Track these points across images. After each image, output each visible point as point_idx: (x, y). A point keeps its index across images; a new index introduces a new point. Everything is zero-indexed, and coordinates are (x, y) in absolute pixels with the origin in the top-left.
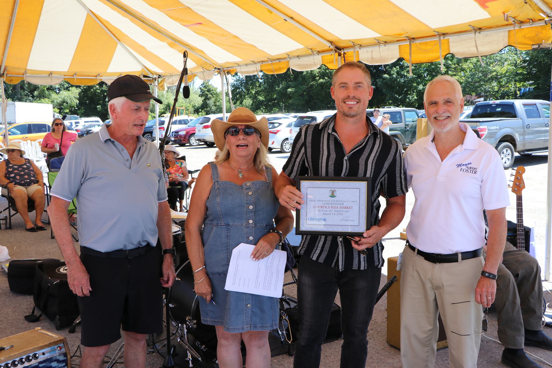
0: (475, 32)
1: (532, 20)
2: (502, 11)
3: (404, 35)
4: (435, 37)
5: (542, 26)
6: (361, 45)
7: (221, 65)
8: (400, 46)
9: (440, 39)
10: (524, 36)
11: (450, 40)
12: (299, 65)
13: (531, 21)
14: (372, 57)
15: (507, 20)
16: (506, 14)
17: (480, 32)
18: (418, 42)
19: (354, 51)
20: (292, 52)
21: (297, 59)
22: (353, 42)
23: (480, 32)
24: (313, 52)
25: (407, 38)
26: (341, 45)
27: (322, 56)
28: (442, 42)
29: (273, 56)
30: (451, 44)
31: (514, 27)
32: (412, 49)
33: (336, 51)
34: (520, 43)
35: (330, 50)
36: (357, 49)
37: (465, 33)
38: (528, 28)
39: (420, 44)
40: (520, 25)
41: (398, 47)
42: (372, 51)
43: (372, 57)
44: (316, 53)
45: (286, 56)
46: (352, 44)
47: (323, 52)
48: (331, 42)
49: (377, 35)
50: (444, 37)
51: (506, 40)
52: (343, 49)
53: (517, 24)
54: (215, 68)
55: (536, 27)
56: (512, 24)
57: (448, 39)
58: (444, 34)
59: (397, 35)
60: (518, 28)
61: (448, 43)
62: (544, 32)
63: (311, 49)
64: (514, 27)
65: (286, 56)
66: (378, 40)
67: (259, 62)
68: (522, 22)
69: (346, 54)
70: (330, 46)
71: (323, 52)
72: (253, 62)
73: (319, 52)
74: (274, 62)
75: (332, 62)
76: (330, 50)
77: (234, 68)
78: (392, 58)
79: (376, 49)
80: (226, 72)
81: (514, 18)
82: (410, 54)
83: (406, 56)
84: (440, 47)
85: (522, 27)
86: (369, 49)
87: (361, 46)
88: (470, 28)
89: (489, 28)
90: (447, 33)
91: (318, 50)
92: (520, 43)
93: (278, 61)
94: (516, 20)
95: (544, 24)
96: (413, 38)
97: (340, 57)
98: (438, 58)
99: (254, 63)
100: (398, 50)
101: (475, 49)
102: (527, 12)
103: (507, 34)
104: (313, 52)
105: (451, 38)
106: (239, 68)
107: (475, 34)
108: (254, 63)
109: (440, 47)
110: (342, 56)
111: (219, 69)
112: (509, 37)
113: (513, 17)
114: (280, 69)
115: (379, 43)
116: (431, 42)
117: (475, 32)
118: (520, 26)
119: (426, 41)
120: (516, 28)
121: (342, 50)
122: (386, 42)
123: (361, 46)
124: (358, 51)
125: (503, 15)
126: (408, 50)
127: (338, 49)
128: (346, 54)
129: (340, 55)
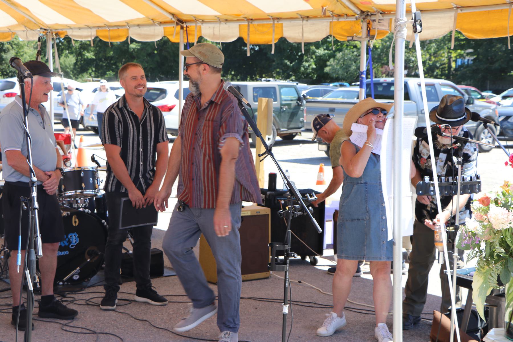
0: (303, 20)
1: (347, 15)
2: (321, 5)
3: (242, 16)
4: (268, 20)
5: (354, 21)
6: (203, 21)
7: (49, 26)
8: (240, 25)
9: (274, 23)
10: (342, 28)
11: (284, 25)
12: (139, 35)
13: (345, 16)
14: (214, 34)
15: (324, 13)
16: (324, 8)
17: (307, 20)
18: (255, 23)
19: (196, 26)
20: (132, 20)
21: (137, 28)
22: (195, 17)
23: (307, 20)
24: (153, 22)
25: (246, 19)
26: (184, 18)
27: (164, 28)
28: (275, 25)
29: (111, 23)
30: (284, 29)
32: (251, 30)
33: (177, 24)
34: (339, 34)
35: (171, 22)
36: (199, 24)
37: (297, 20)
38: (345, 21)
39: (258, 25)
40: (337, 18)
41: (238, 26)
42: (214, 28)
43: (214, 34)
44: (158, 24)
45: (126, 24)
46: (194, 19)
47: (165, 23)
48: (173, 15)
49: (217, 14)
50: (278, 22)
51: (328, 30)
52: (185, 22)
53: (335, 17)
54: (41, 28)
55: (351, 21)
56: (329, 16)
57: (282, 24)
58: (278, 19)
59: (235, 15)
60: (336, 20)
61: (282, 27)
62: (357, 26)
63: (152, 20)
64: (333, 19)
65: (126, 24)
66: (218, 18)
67: (94, 27)
68: (339, 16)
69: (188, 27)
70: (171, 19)
71: (165, 23)
72: (88, 26)
73: (161, 23)
74: (111, 28)
75: (172, 35)
76: (171, 22)
77: (64, 30)
78: (233, 37)
79: (217, 25)
80: (54, 34)
81: (332, 11)
82: (248, 35)
83: (245, 37)
84: (274, 30)
85: (340, 20)
86: (212, 25)
87: (203, 21)
88: (300, 17)
89: (315, 17)
90: (281, 18)
91: (160, 20)
92: (339, 34)
93: (116, 28)
95: (355, 19)
96: (252, 19)
97: (182, 31)
98: (271, 41)
99: (89, 27)
100: (237, 29)
101: (301, 35)
102: (339, 9)
103: (329, 24)
104: (153, 22)
105: (285, 23)
106: (71, 30)
108: (89, 27)
109: (274, 30)
110: (185, 29)
111: (45, 30)
112: (330, 27)
113: (331, 10)
114: (119, 37)
115: (219, 20)
117: (303, 20)
118: (338, 19)
119: (263, 23)
120: (334, 20)
121: (184, 23)
122: (227, 20)
123: (203, 21)
124: (200, 26)
125: (321, 7)
126: (247, 30)
127: (180, 22)
128: (188, 27)
129: (182, 28)
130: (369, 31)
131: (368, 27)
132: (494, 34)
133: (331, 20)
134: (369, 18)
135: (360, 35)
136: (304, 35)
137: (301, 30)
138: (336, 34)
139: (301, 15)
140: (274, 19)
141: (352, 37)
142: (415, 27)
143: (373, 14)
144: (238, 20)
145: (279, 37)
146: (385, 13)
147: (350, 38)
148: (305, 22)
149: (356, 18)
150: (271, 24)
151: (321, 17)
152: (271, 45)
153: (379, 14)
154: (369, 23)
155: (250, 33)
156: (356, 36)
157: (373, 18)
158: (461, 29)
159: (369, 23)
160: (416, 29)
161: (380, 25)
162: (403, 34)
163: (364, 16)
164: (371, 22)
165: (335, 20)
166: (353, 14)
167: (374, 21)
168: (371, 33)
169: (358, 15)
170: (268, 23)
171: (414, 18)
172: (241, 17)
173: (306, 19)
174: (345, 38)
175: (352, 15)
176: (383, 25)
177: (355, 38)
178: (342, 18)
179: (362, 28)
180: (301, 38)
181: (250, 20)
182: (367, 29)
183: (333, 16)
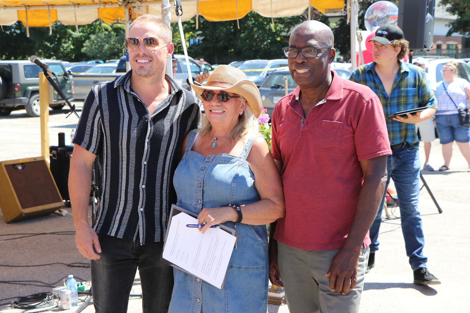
0: (75, 7)
1: (111, 2)
3: (20, 3)
4: (44, 7)
5: (118, 7)
8: (18, 11)
10: (108, 13)
11: (58, 10)
13: (110, 3)
17: (78, 7)
18: (32, 9)
23: (78, 7)
25: (23, 6)
30: (58, 14)
31: (100, 6)
32: (29, 14)
34: (106, 18)
38: (110, 8)
39: (34, 10)
40: (104, 5)
50: (53, 8)
51: (97, 15)
53: (102, 4)
55: (115, 8)
56: (97, 4)
57: (56, 10)
64: (100, 6)
68: (105, 3)
82: (27, 19)
83: (24, 21)
84: (50, 15)
85: (106, 7)
88: (71, 4)
89: (85, 4)
90: (55, 5)
92: (106, 18)
94: (101, 1)
95: (118, 6)
96: (29, 6)
98: (48, 24)
100: (16, 14)
101: (74, 19)
103: (97, 10)
105: (59, 9)
107: (75, 8)
109: (50, 15)
112: (98, 12)
116: (43, 10)
117: (75, 7)
118: (104, 6)
122: (5, 6)
126: (24, 15)
130: (130, 16)
131: (130, 12)
132: (227, 18)
133: (99, 7)
134: (130, 5)
135: (124, 19)
136: (77, 19)
137: (74, 15)
138: (103, 18)
139: (72, 3)
140: (49, 5)
141: (118, 20)
142: (177, 11)
143: (133, 2)
144: (16, 6)
145: (54, 20)
146: (142, 1)
147: (116, 21)
148: (76, 8)
149: (119, 5)
150: (46, 10)
151: (90, 4)
152: (48, 28)
153: (138, 2)
154: (130, 9)
155: (28, 17)
156: (121, 20)
157: (133, 5)
158: (203, 14)
159: (130, 9)
160: (178, 13)
161: (139, 10)
162: (168, 17)
163: (126, 4)
164: (132, 8)
165: (102, 6)
166: (117, 2)
167: (134, 7)
168: (132, 17)
169: (121, 2)
170: (44, 9)
171: (176, 5)
172: (19, 4)
173: (77, 6)
174: (111, 21)
175: (116, 3)
176: (142, 11)
177: (120, 21)
178: (108, 5)
179: (125, 13)
180: (74, 21)
181: (28, 6)
182: (129, 14)
183: (100, 3)
